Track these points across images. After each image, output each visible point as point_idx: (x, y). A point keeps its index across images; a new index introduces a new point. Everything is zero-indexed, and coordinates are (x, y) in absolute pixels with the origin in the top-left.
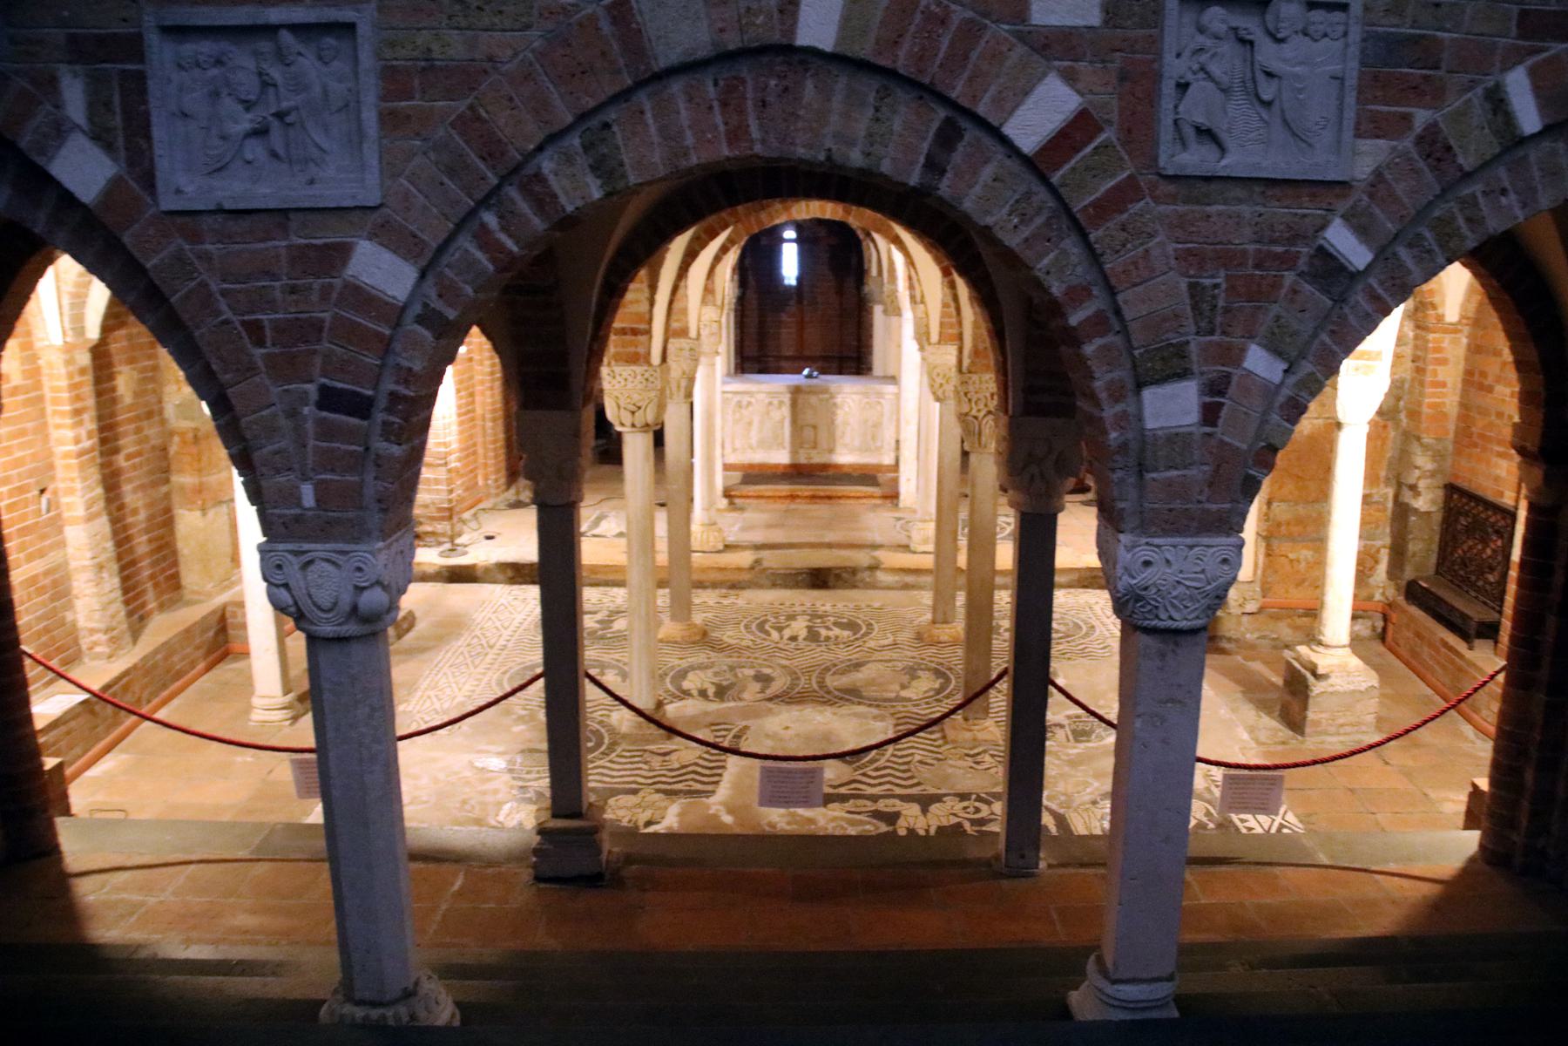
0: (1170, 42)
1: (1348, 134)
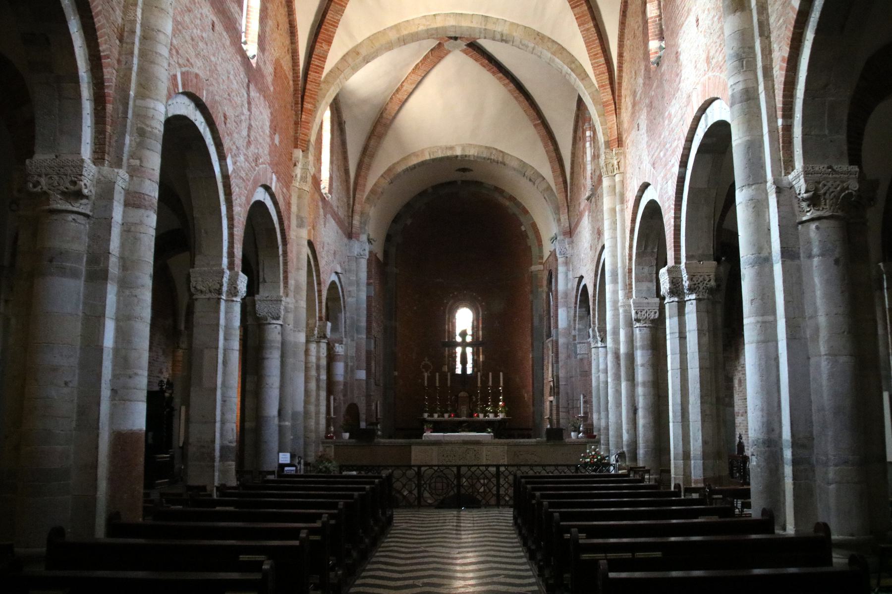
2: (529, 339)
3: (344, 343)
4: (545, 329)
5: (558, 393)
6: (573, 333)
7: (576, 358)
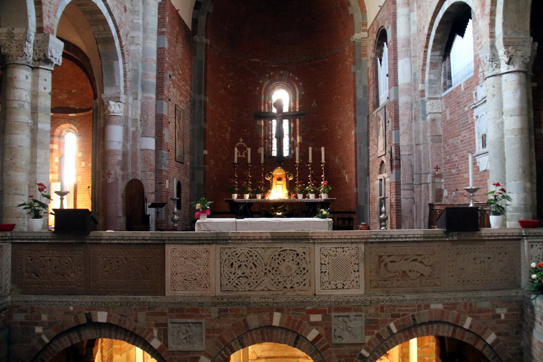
0: (333, 323)
1: (363, 336)
2: (351, 114)
3: (121, 100)
4: (372, 99)
5: (398, 167)
6: (420, 87)
7: (424, 119)
